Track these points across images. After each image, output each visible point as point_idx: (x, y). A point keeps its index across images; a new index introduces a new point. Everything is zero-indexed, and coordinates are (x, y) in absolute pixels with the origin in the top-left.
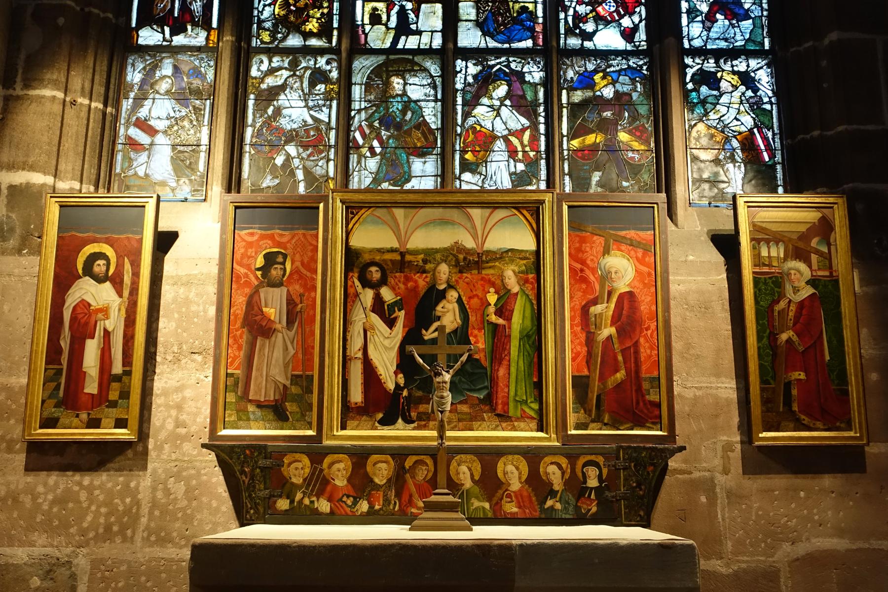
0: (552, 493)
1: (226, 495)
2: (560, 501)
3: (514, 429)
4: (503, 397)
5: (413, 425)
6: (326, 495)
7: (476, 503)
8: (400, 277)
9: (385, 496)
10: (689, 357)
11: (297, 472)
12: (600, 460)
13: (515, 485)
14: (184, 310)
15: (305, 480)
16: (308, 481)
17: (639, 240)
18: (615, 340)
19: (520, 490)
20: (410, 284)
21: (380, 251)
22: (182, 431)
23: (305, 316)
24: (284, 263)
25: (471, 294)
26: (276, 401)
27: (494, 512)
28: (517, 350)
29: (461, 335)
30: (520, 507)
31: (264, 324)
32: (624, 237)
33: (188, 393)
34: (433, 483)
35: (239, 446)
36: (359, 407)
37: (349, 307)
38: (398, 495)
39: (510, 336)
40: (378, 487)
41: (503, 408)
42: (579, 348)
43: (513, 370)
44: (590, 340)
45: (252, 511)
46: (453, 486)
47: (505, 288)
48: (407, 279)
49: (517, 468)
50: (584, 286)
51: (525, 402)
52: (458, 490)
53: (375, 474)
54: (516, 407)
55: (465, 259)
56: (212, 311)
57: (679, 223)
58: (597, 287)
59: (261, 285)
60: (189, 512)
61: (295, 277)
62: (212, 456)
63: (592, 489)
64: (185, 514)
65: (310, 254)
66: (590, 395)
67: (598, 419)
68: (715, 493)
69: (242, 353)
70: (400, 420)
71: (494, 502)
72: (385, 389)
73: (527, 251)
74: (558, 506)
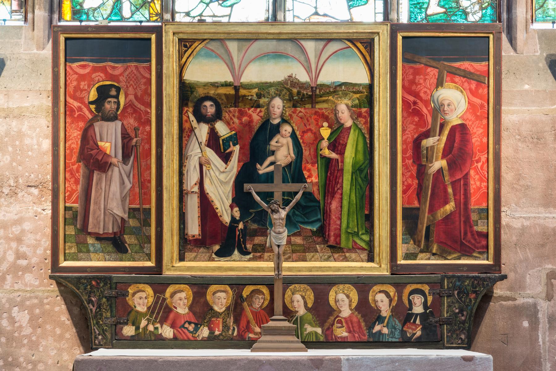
0: (380, 319)
1: (69, 323)
2: (387, 326)
3: (346, 259)
4: (335, 229)
5: (248, 257)
6: (169, 321)
7: (309, 329)
8: (235, 112)
9: (224, 322)
10: (519, 187)
11: (141, 301)
12: (426, 288)
13: (346, 312)
14: (17, 143)
15: (149, 308)
16: (151, 310)
17: (472, 71)
18: (446, 173)
19: (350, 317)
20: (245, 119)
21: (215, 85)
22: (23, 262)
23: (140, 150)
24: (117, 97)
25: (305, 129)
26: (115, 233)
27: (326, 336)
28: (349, 183)
29: (294, 172)
30: (349, 332)
31: (100, 158)
32: (458, 69)
33: (27, 226)
34: (270, 310)
35: (85, 278)
36: (196, 240)
37: (185, 142)
38: (237, 321)
39: (342, 170)
40: (217, 315)
41: (335, 240)
42: (410, 181)
43: (345, 203)
44: (421, 173)
45: (100, 337)
46: (288, 313)
47: (338, 122)
48: (242, 113)
49: (348, 296)
50: (416, 119)
51: (357, 234)
52: (293, 317)
53: (214, 303)
54: (347, 239)
55: (299, 93)
56: (47, 144)
57: (518, 48)
58: (430, 119)
59: (95, 119)
60: (34, 338)
61: (129, 110)
62: (54, 287)
63: (417, 315)
64: (30, 341)
65: (143, 87)
66: (420, 226)
67: (427, 249)
68: (537, 319)
69: (79, 188)
70: (236, 252)
71: (326, 328)
72: (221, 222)
73: (360, 85)
74: (385, 331)
